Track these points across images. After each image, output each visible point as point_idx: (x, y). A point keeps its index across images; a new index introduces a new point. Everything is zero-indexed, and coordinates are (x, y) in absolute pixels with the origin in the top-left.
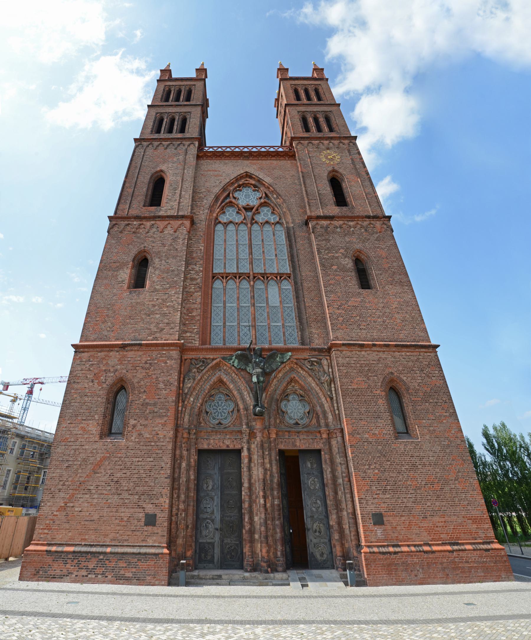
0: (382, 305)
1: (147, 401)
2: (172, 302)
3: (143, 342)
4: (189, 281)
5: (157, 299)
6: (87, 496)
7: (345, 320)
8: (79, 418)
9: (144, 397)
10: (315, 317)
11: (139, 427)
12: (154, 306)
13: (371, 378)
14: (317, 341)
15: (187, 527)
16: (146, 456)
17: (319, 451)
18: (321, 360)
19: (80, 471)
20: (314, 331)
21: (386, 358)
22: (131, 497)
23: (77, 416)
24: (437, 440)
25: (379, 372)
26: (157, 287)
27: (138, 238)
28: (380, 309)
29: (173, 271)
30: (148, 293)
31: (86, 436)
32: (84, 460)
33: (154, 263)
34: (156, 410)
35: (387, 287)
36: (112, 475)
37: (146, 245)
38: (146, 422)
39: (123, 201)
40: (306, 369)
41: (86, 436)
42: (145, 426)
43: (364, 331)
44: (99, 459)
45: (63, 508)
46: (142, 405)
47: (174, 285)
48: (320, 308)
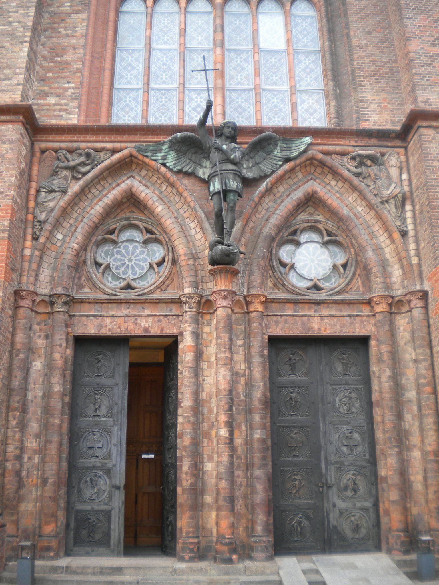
10: (372, 68)
15: (45, 481)
18: (383, 155)
40: (346, 173)
48: (386, 50)
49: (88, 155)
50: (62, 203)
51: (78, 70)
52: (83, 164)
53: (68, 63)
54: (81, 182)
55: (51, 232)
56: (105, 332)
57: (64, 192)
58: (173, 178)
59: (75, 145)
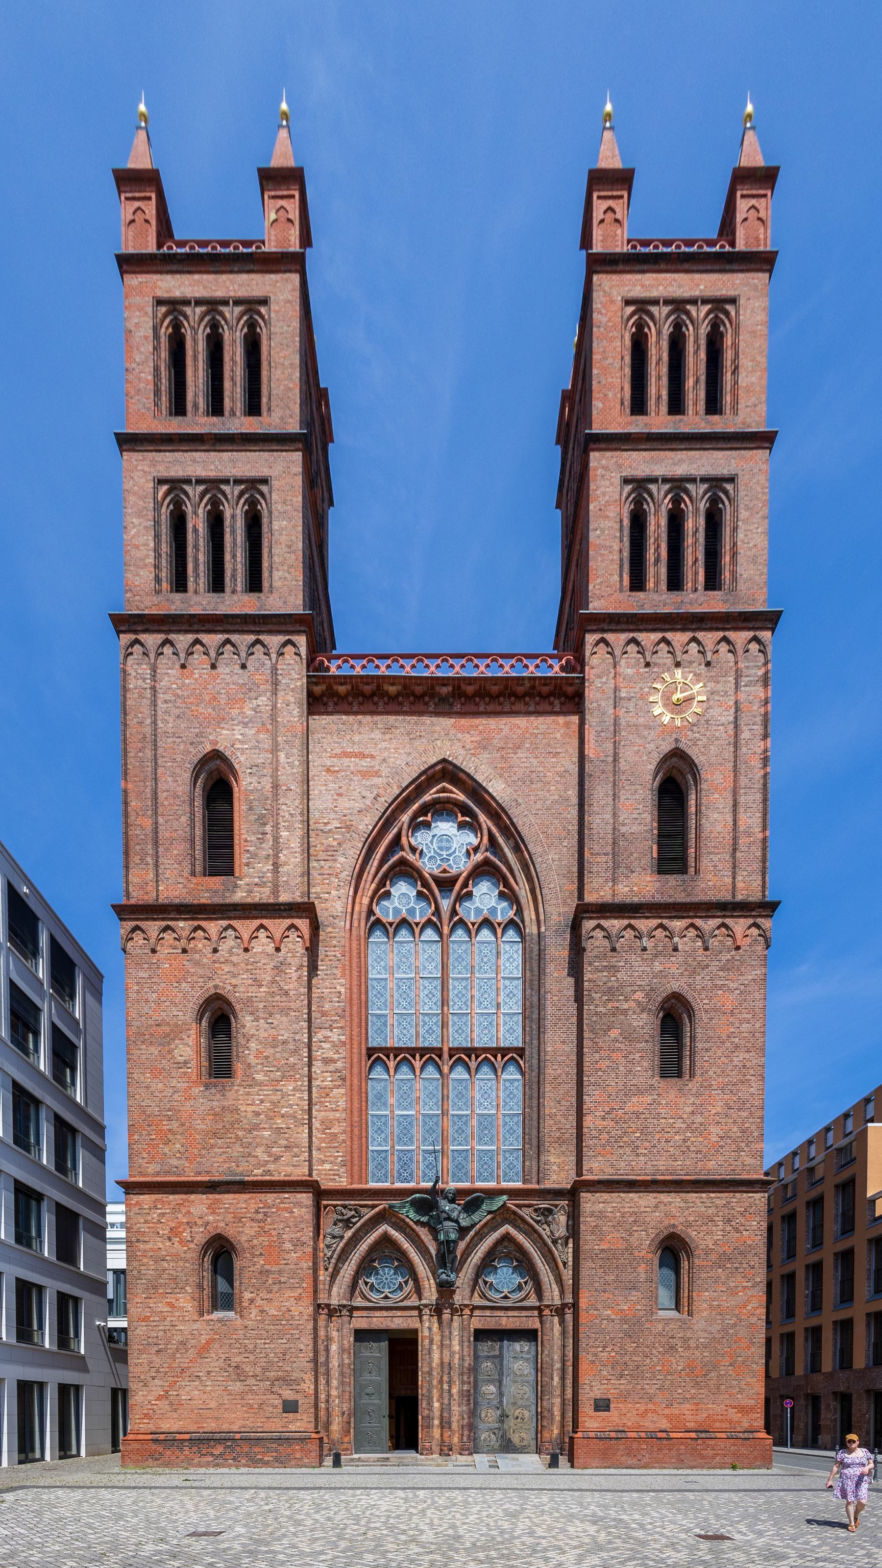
0: (689, 1109)
1: (267, 1267)
2: (291, 1106)
3: (246, 1178)
4: (319, 1064)
5: (262, 1101)
6: (197, 1383)
7: (612, 1140)
8: (161, 1291)
9: (262, 1262)
11: (259, 1302)
12: (257, 1114)
13: (636, 1234)
14: (555, 1177)
16: (275, 1336)
17: (536, 1331)
19: (178, 1355)
20: (552, 1160)
21: (670, 1203)
22: (262, 1384)
23: (155, 1288)
24: (719, 1317)
25: (652, 1224)
26: (259, 1077)
27: (197, 963)
28: (685, 1116)
29: (284, 1042)
30: (242, 1089)
31: (177, 1314)
32: (183, 1343)
33: (244, 1027)
34: (283, 1280)
35: (711, 1073)
36: (227, 1359)
37: (217, 982)
38: (269, 1296)
39: (137, 859)
41: (177, 1314)
42: (269, 1300)
43: (642, 1158)
44: (204, 1342)
45: (166, 1396)
46: (261, 1273)
47: (292, 1073)
49: (355, 1210)
50: (341, 1245)
51: (344, 1141)
52: (353, 1217)
53: (335, 1135)
54: (353, 1230)
55: (336, 1265)
56: (373, 1327)
57: (342, 1237)
58: (414, 1226)
59: (347, 1202)
